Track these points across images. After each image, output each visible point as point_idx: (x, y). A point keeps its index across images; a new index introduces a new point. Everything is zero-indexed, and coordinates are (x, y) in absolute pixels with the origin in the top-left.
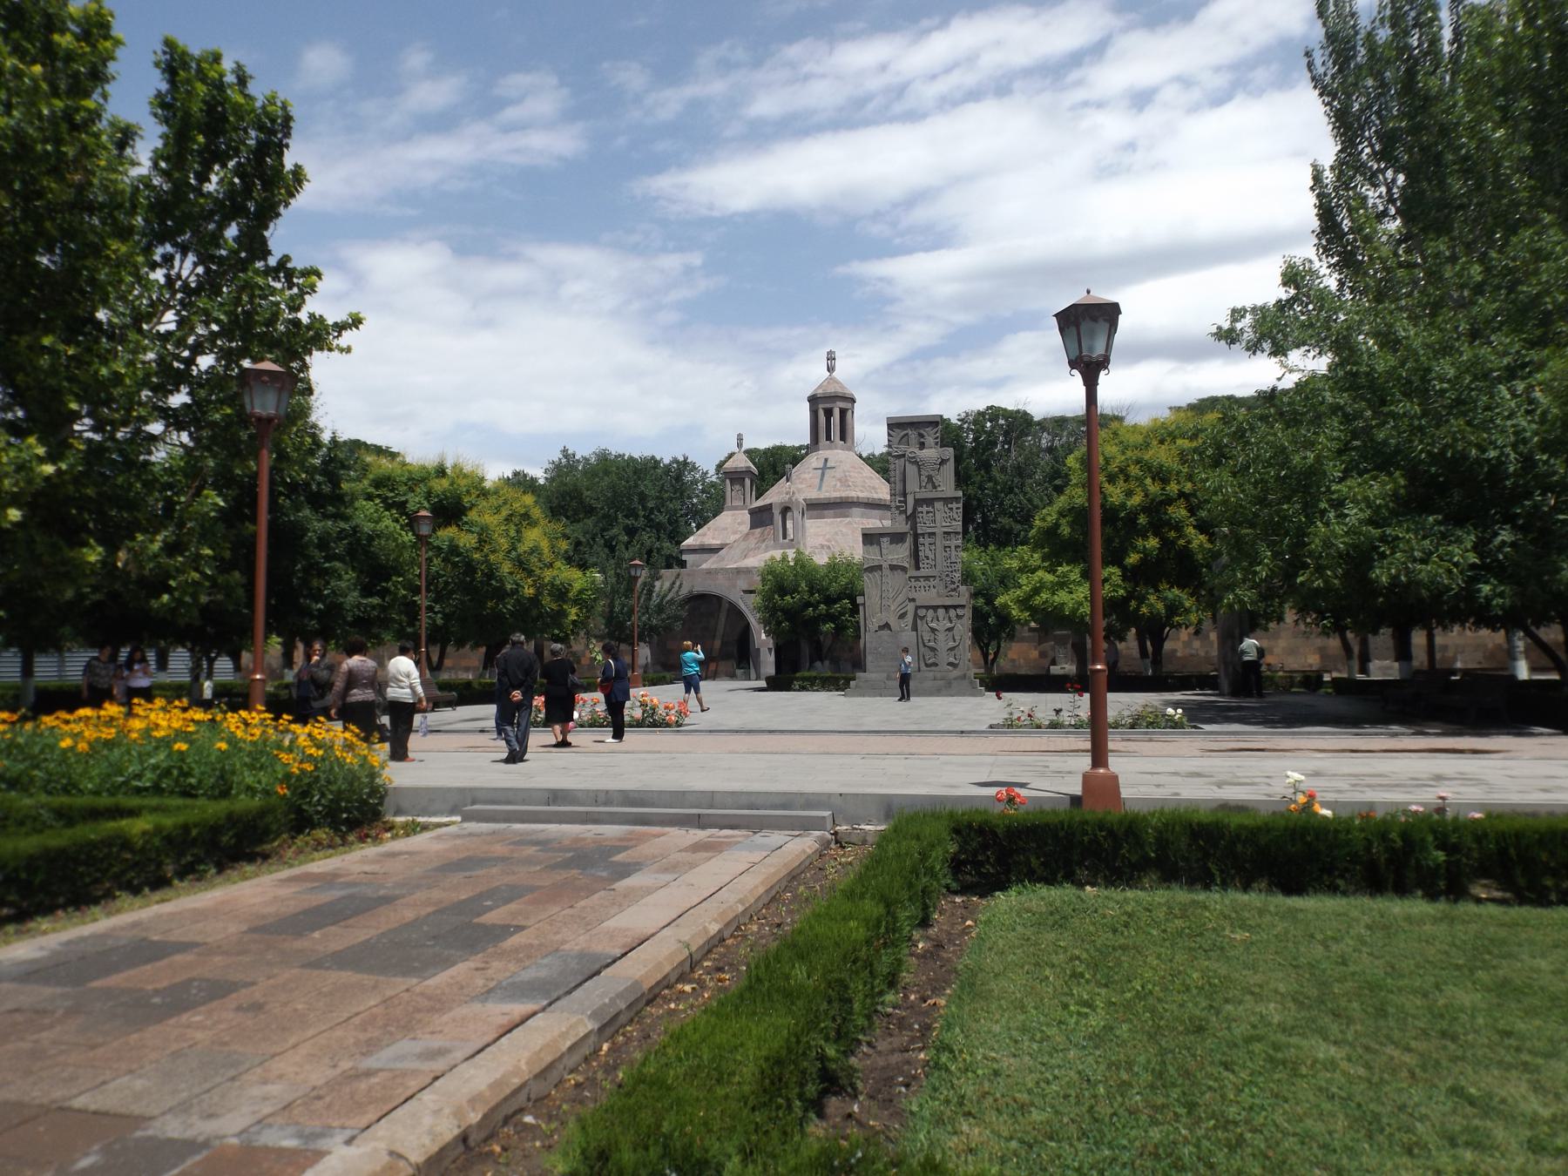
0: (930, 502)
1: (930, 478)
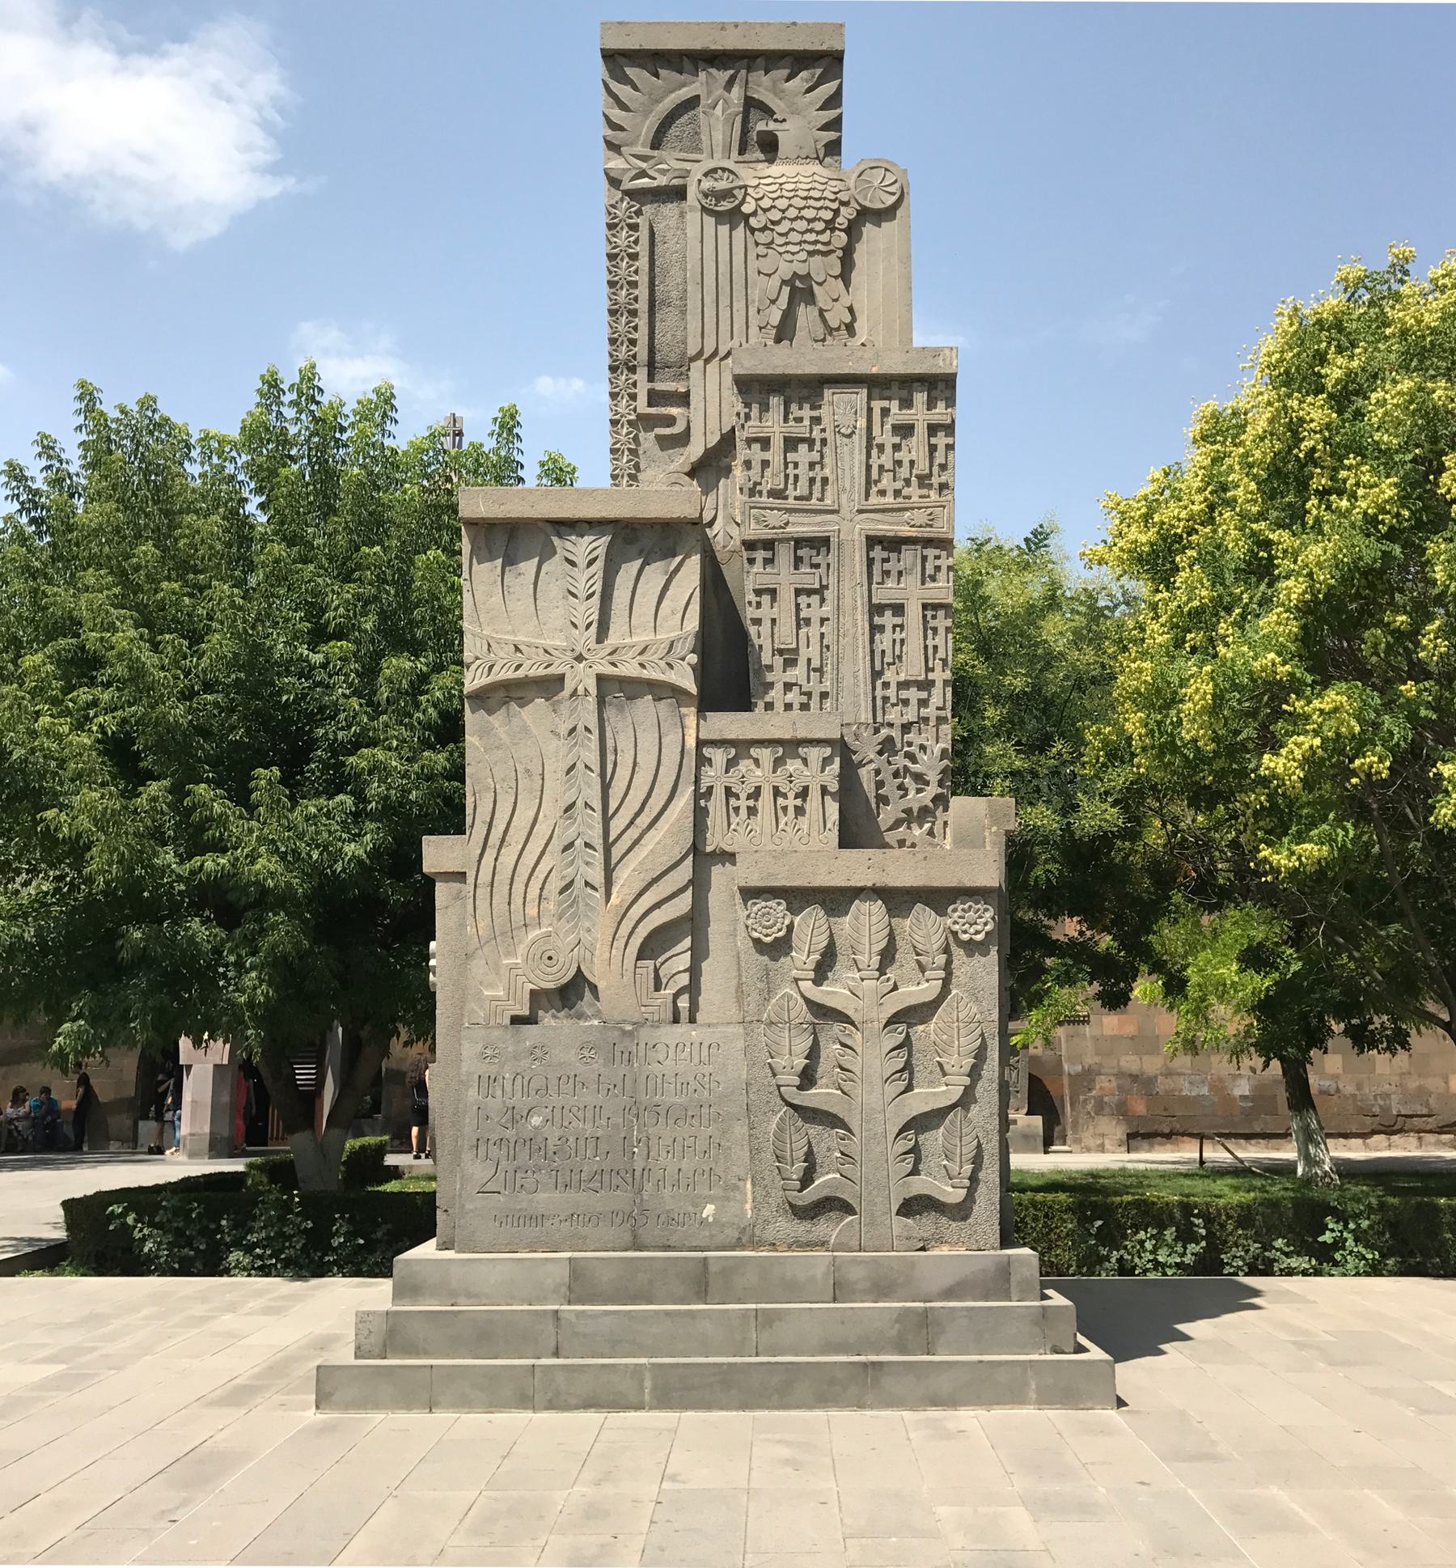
0: (808, 389)
1: (801, 290)
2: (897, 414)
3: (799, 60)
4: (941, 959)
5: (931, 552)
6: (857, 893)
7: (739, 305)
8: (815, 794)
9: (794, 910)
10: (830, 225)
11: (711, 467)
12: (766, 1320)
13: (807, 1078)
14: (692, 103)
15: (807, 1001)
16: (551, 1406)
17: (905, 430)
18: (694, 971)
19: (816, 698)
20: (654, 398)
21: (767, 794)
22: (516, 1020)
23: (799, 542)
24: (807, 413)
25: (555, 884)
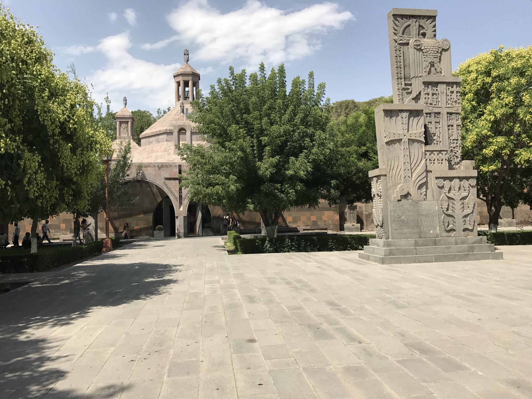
0: (435, 84)
1: (432, 65)
2: (451, 89)
3: (429, 17)
4: (468, 189)
5: (457, 115)
6: (454, 178)
7: (421, 67)
8: (444, 160)
9: (444, 181)
10: (437, 52)
11: (417, 99)
12: (448, 248)
13: (448, 210)
14: (409, 26)
15: (447, 196)
16: (419, 262)
17: (452, 92)
18: (426, 192)
19: (438, 143)
20: (406, 85)
21: (436, 160)
22: (398, 200)
23: (435, 113)
24: (435, 88)
25: (403, 177)
